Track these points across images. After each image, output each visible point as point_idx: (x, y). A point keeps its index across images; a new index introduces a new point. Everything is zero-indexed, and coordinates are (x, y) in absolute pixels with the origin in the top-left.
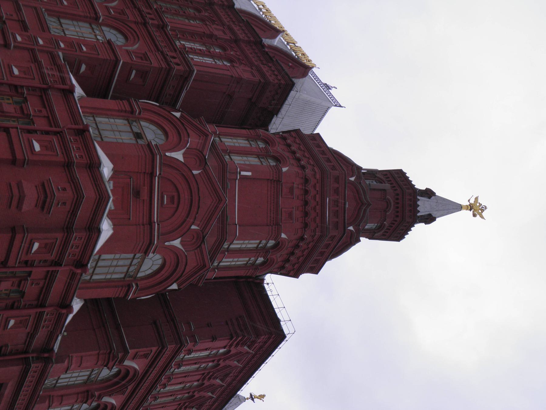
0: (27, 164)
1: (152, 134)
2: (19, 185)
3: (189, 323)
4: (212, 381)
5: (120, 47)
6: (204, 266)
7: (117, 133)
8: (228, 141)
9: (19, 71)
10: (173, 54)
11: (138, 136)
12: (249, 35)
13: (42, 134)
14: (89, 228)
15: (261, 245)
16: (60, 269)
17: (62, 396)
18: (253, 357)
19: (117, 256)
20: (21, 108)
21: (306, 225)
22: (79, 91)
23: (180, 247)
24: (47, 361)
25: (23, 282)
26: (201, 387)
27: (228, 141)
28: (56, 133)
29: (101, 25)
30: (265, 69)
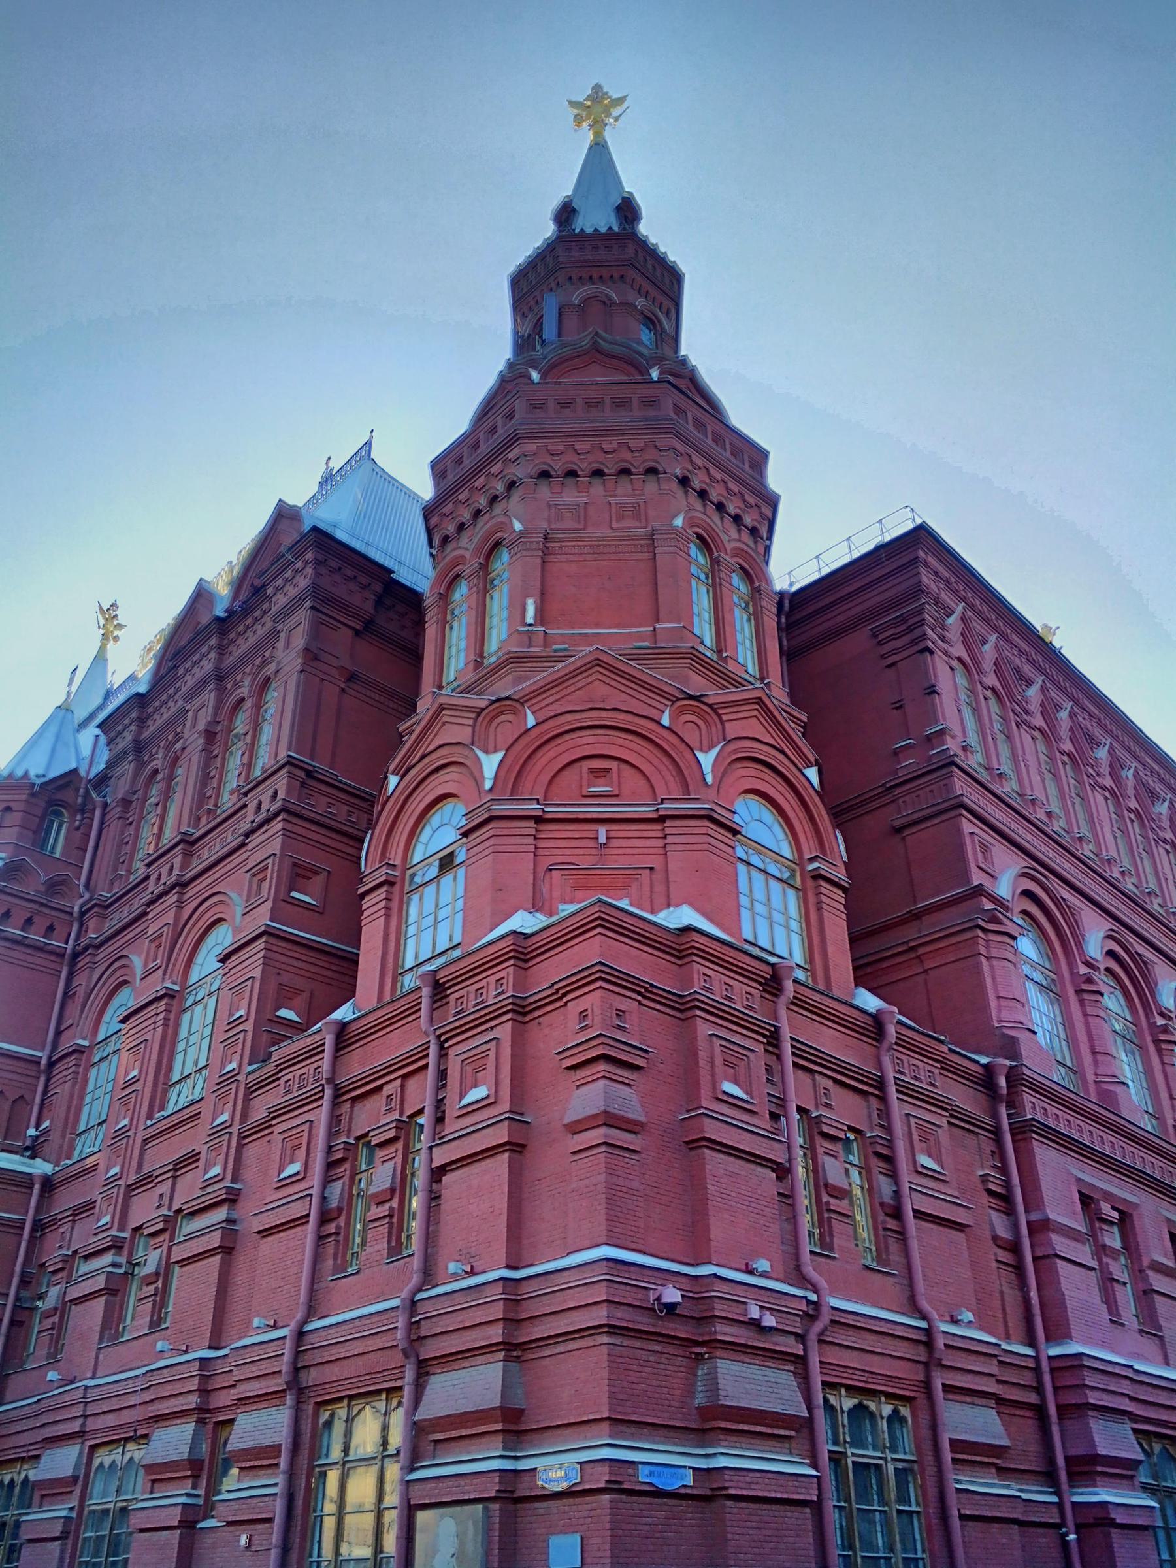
0: (522, 1114)
1: (442, 832)
2: (575, 1128)
3: (896, 752)
4: (1034, 707)
5: (236, 931)
6: (759, 701)
7: (442, 914)
8: (457, 662)
9: (292, 1162)
10: (252, 806)
11: (447, 863)
12: (204, 649)
13: (445, 1086)
14: (679, 958)
15: (703, 577)
16: (786, 1034)
17: (1094, 1053)
18: (972, 607)
19: (744, 900)
20: (382, 1145)
21: (652, 471)
22: (344, 1013)
23: (714, 753)
24: (1015, 1077)
25: (825, 1129)
26: (1049, 735)
27: (457, 662)
28: (443, 1053)
29: (184, 986)
30: (281, 600)
